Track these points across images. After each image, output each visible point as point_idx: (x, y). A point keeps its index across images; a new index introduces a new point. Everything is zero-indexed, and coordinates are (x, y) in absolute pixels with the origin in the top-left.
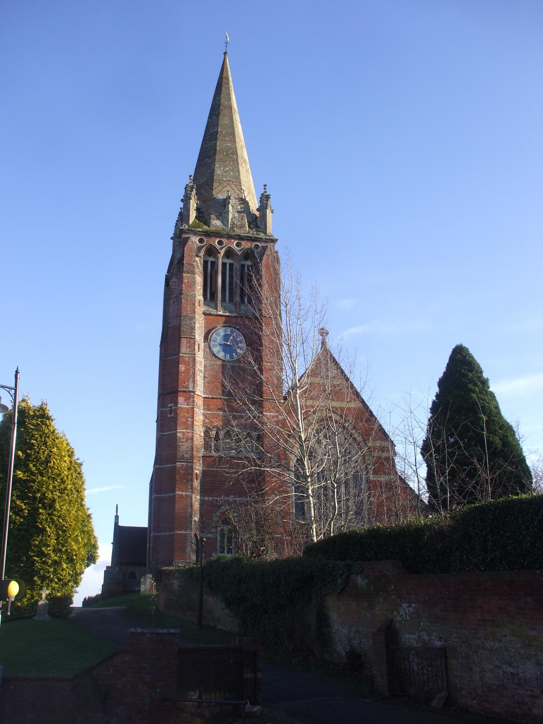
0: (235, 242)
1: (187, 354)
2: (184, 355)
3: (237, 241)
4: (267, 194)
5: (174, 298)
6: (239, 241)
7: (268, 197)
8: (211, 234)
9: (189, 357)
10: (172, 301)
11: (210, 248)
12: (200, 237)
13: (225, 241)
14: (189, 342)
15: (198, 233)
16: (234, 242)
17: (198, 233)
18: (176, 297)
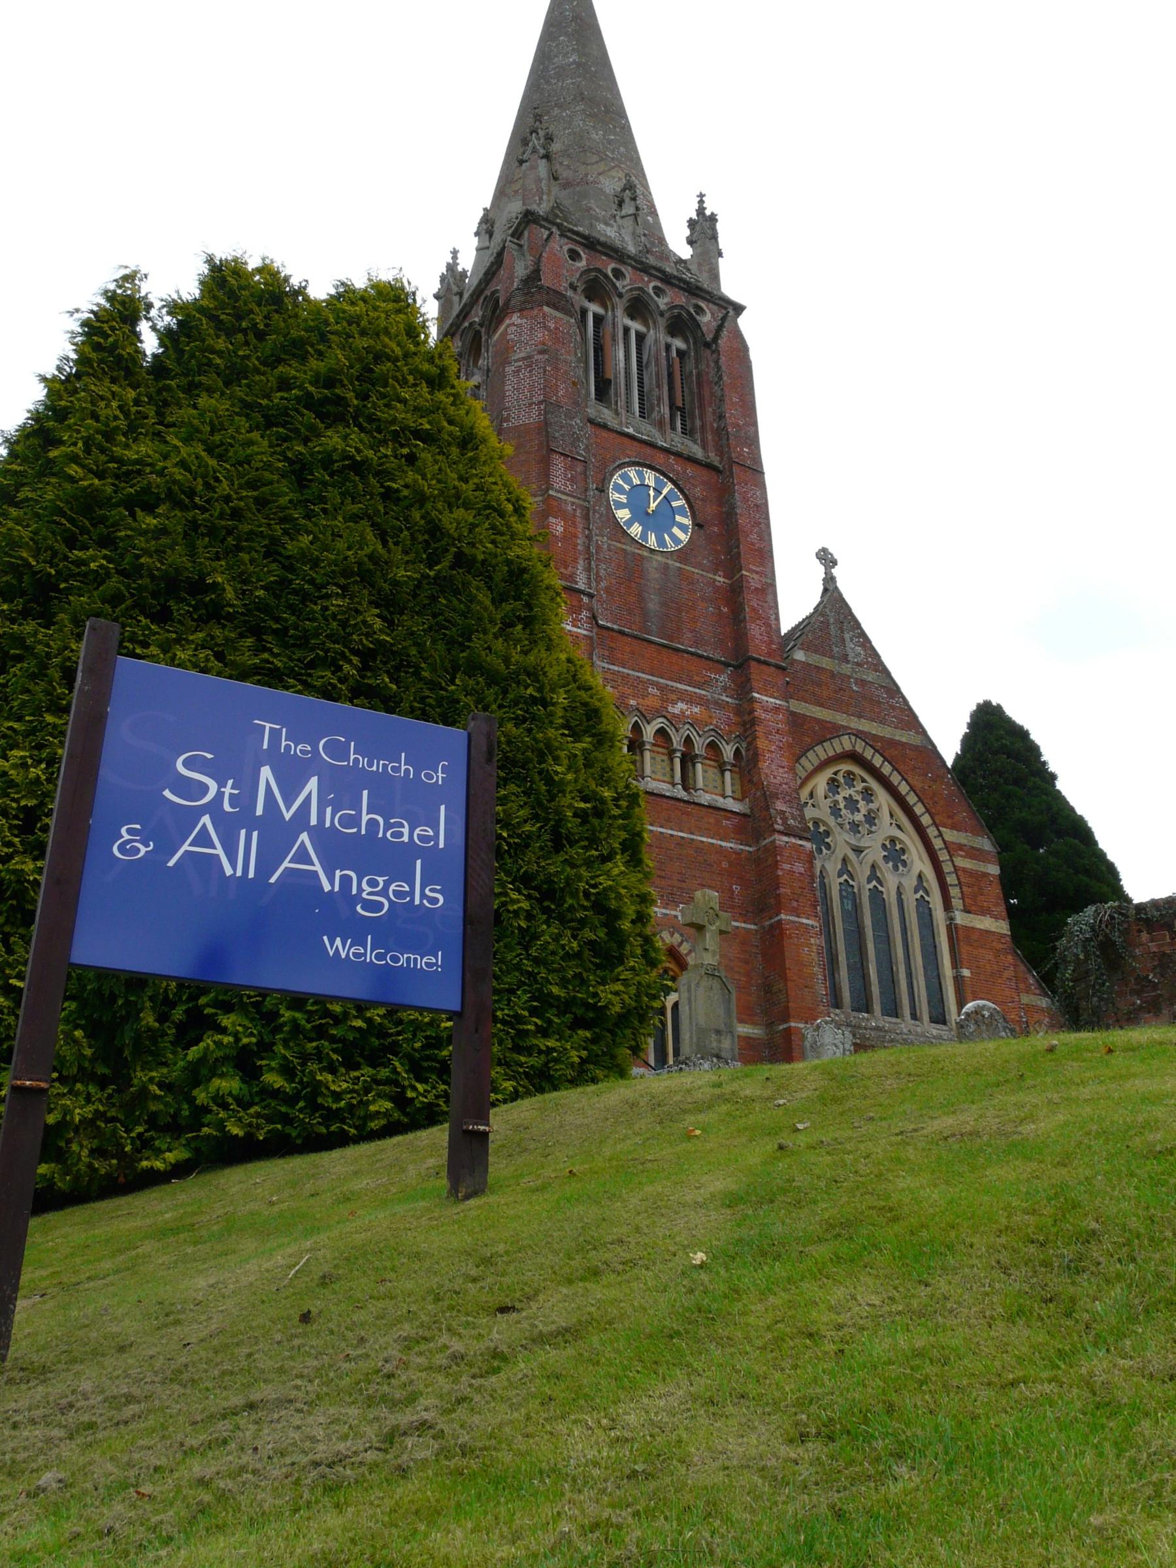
0: (652, 285)
1: (568, 495)
2: (564, 497)
3: (659, 284)
4: (708, 213)
5: (516, 361)
6: (659, 284)
7: (713, 219)
8: (599, 248)
9: (573, 504)
10: (509, 369)
11: (596, 279)
12: (570, 246)
13: (627, 271)
14: (571, 468)
15: (569, 234)
16: (649, 282)
17: (569, 234)
18: (524, 359)
